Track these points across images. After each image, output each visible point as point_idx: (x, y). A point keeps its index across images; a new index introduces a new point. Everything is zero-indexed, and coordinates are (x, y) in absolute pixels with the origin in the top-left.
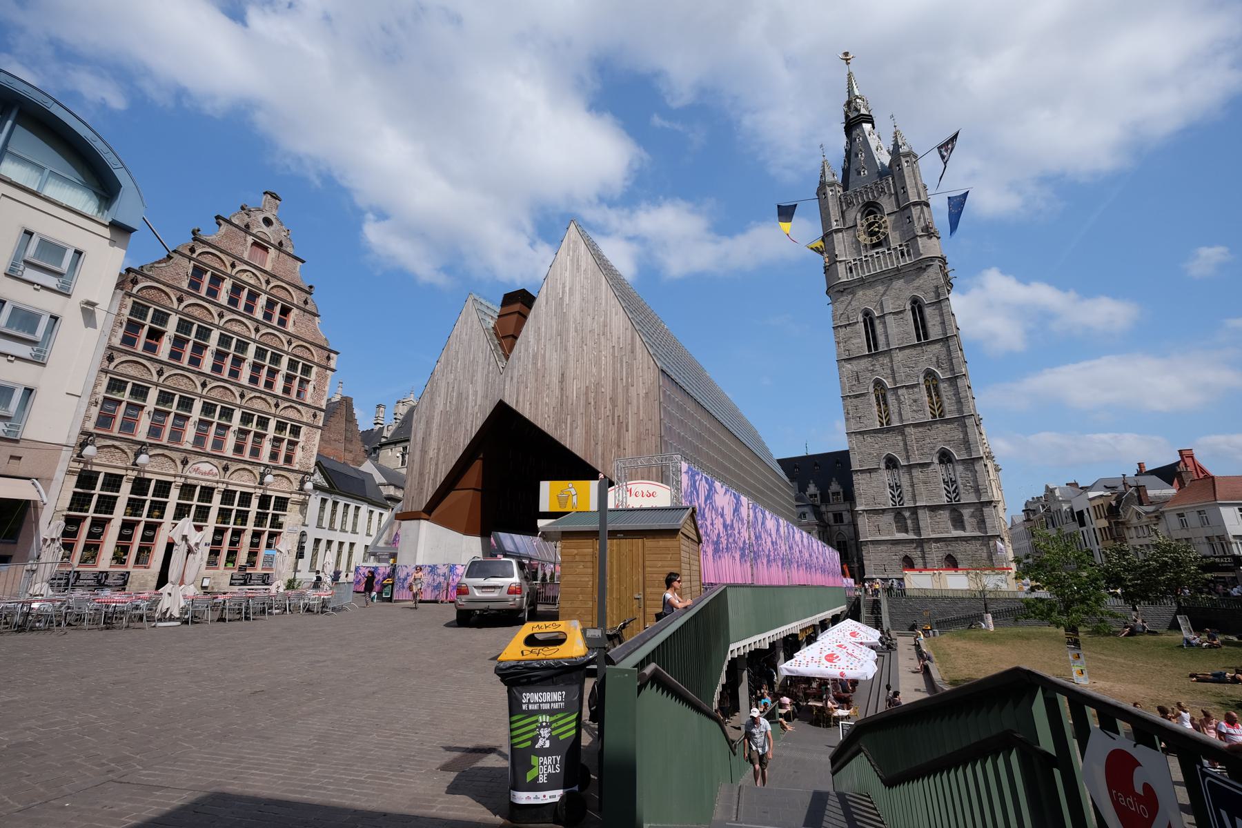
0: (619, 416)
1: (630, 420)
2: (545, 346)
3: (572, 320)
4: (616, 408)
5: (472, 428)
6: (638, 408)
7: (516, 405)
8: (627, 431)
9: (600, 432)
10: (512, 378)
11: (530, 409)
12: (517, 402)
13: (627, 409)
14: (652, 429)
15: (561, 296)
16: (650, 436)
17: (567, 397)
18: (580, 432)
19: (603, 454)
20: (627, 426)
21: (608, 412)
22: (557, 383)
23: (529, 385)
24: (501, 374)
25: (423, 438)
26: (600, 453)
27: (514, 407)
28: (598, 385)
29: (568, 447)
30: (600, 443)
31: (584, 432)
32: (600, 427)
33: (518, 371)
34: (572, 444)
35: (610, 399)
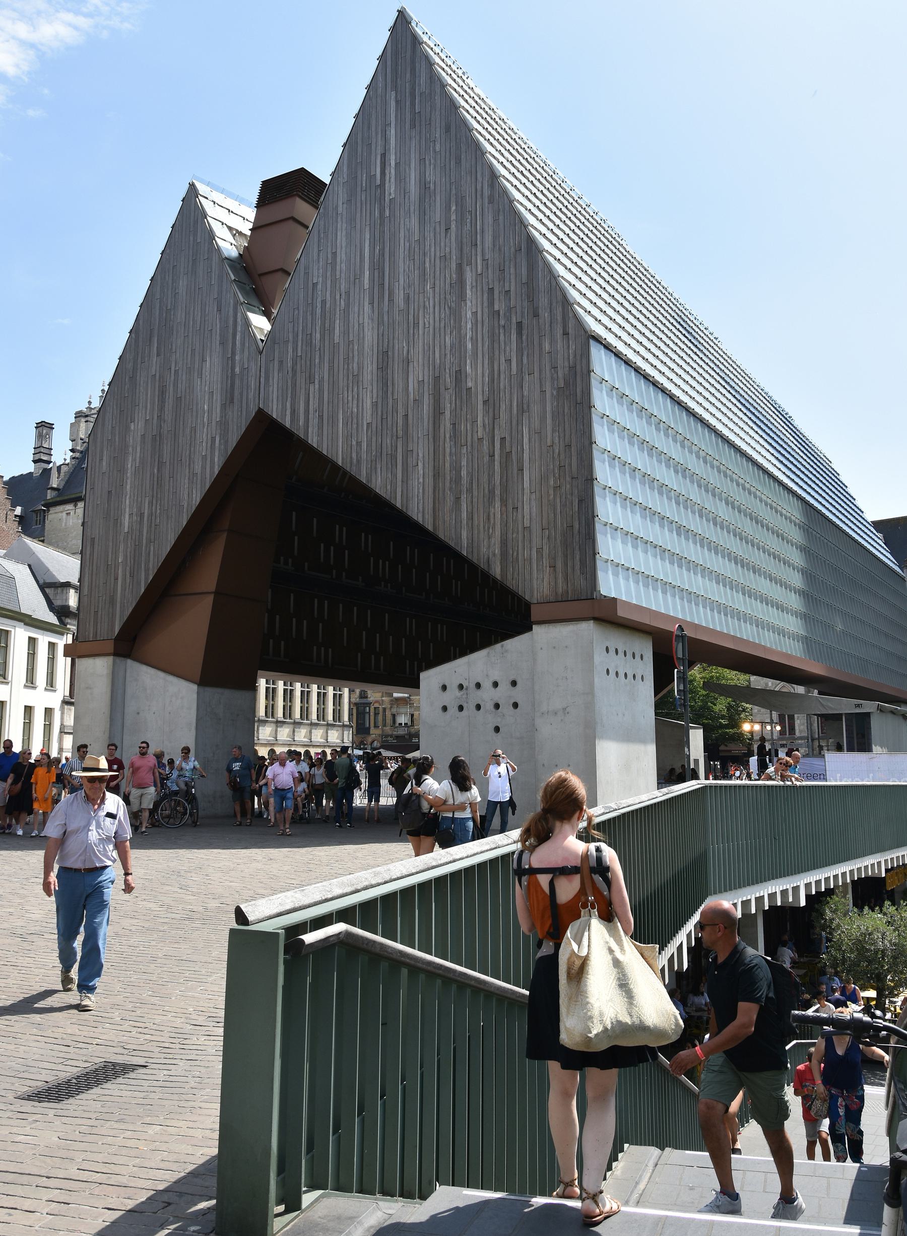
0: (503, 439)
1: (526, 447)
2: (348, 293)
3: (402, 234)
4: (496, 421)
5: (204, 468)
6: (543, 419)
7: (292, 421)
8: (521, 470)
9: (464, 473)
10: (281, 362)
11: (320, 427)
12: (293, 412)
13: (519, 423)
14: (570, 465)
15: (378, 182)
16: (568, 479)
17: (395, 401)
18: (421, 474)
19: (471, 518)
20: (520, 461)
21: (480, 430)
22: (375, 371)
23: (317, 377)
24: (261, 353)
25: (110, 492)
26: (464, 515)
27: (288, 424)
28: (459, 376)
29: (399, 505)
30: (464, 497)
31: (431, 474)
32: (464, 463)
33: (295, 349)
34: (406, 498)
35: (485, 402)
